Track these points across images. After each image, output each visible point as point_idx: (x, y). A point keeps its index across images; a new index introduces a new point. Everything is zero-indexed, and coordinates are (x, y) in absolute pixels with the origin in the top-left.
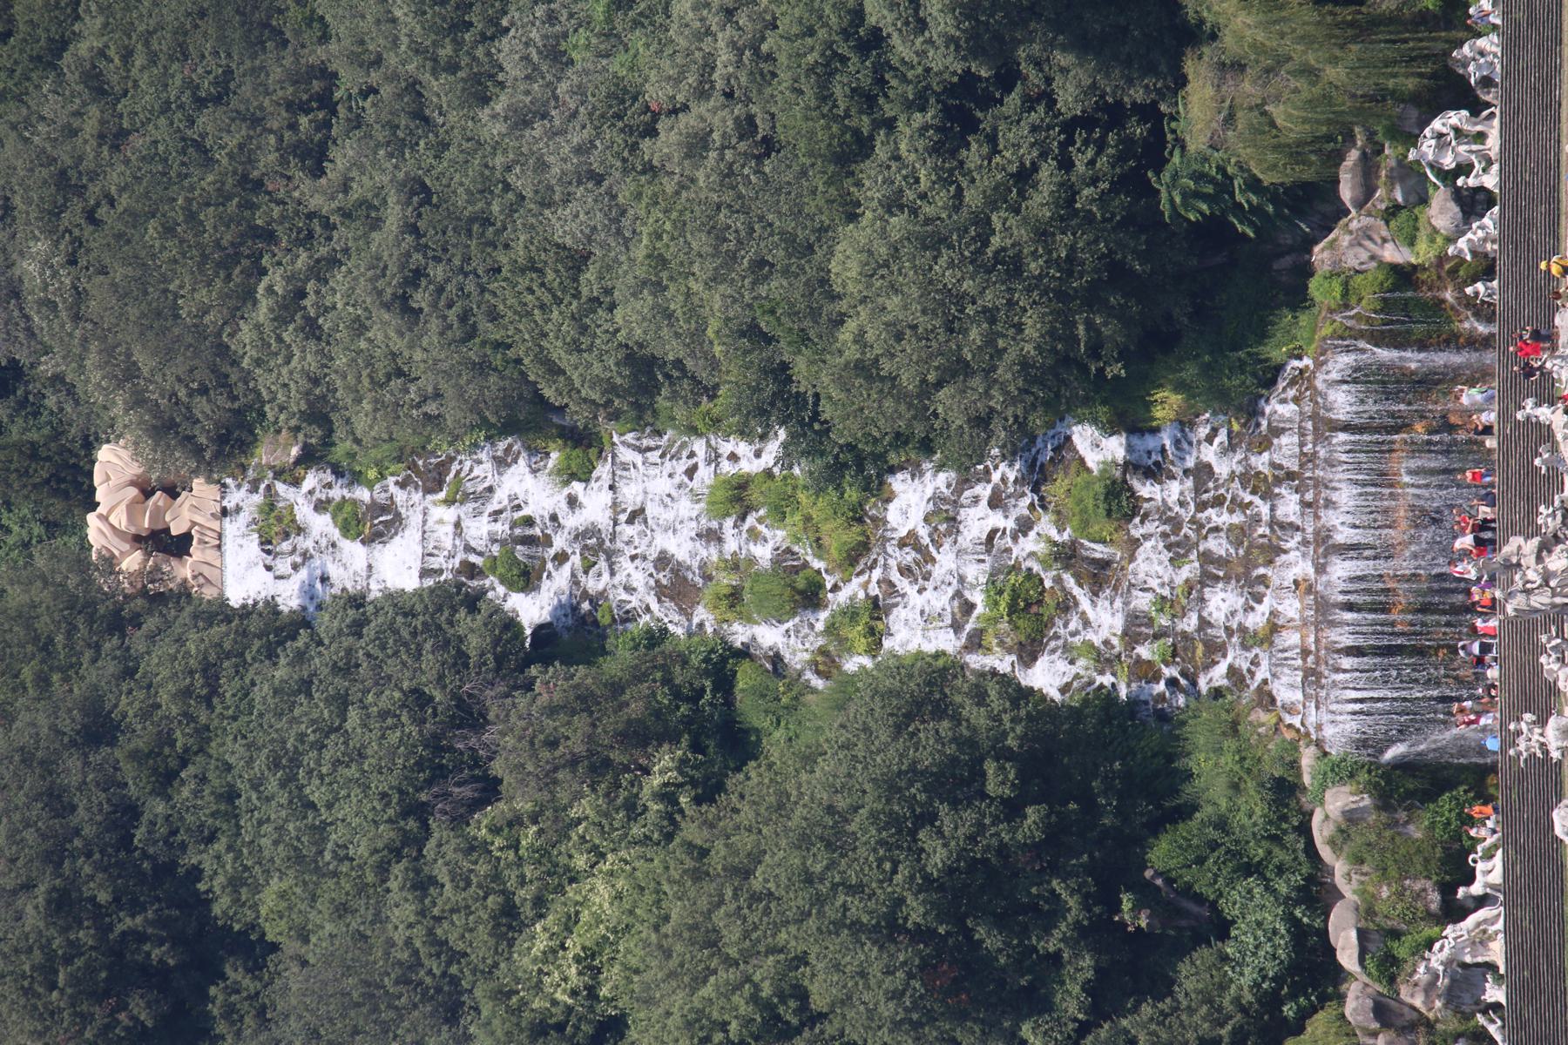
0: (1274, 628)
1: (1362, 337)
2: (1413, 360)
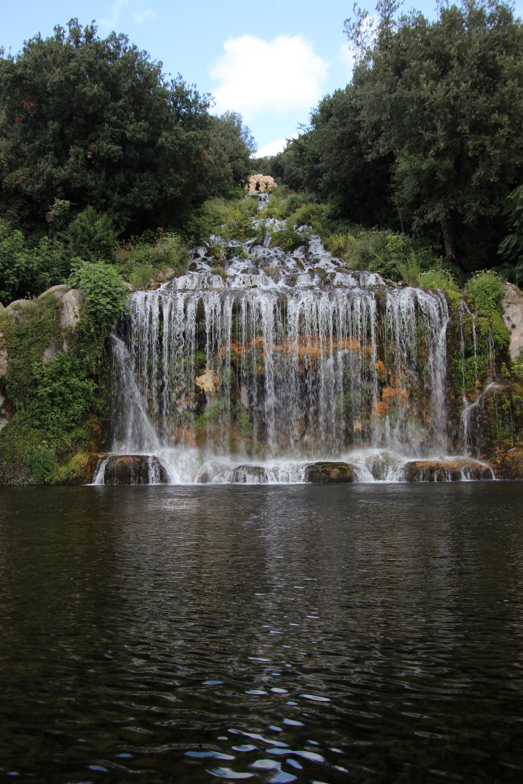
0: (225, 277)
1: (453, 319)
2: (438, 358)
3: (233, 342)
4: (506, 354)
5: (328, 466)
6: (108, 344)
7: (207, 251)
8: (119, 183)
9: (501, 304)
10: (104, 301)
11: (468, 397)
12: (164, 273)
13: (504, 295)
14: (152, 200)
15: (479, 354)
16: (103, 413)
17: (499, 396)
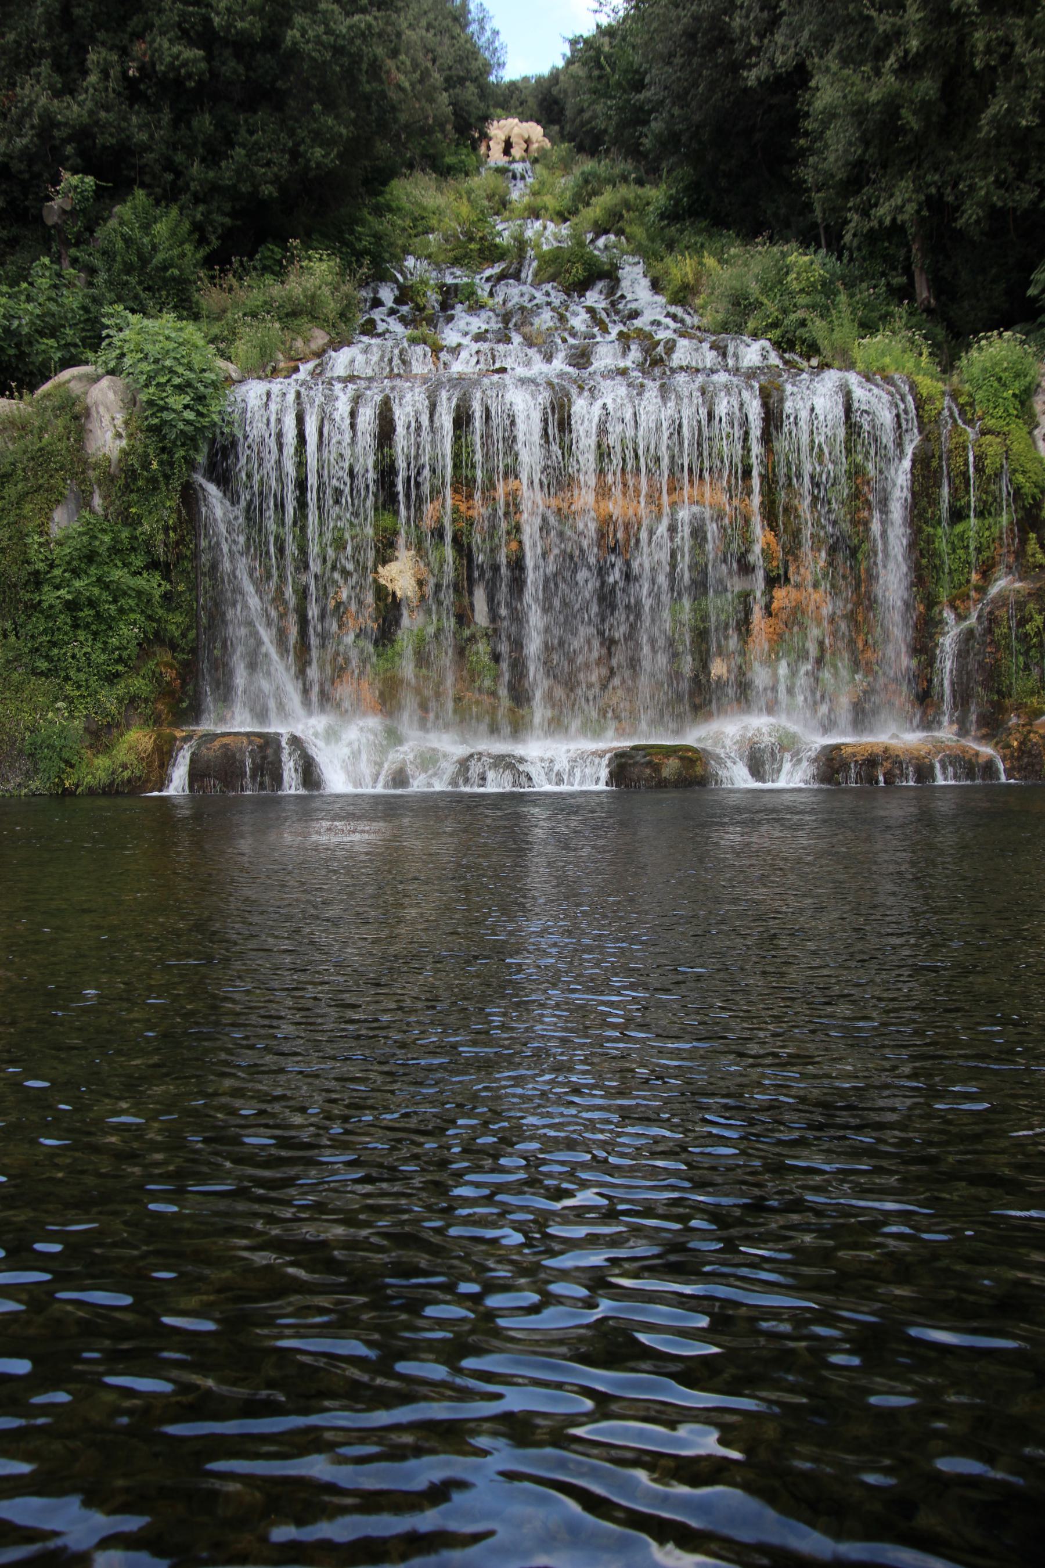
0: (437, 350)
1: (926, 439)
3: (456, 491)
4: (1038, 516)
5: (656, 754)
6: (190, 497)
7: (397, 292)
8: (201, 137)
9: (1031, 407)
10: (177, 401)
11: (954, 607)
12: (307, 341)
13: (1039, 385)
14: (275, 175)
15: (980, 515)
16: (182, 643)
17: (1020, 605)
